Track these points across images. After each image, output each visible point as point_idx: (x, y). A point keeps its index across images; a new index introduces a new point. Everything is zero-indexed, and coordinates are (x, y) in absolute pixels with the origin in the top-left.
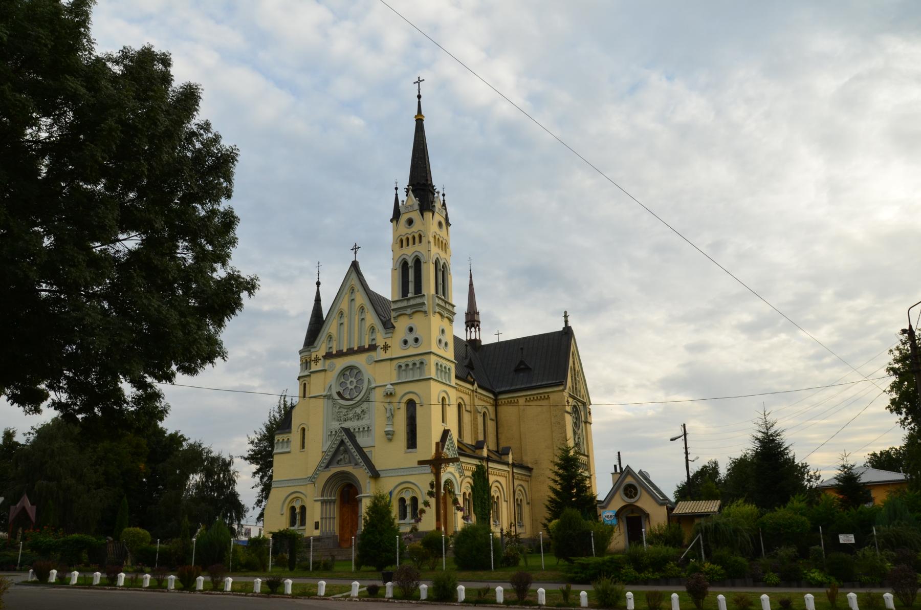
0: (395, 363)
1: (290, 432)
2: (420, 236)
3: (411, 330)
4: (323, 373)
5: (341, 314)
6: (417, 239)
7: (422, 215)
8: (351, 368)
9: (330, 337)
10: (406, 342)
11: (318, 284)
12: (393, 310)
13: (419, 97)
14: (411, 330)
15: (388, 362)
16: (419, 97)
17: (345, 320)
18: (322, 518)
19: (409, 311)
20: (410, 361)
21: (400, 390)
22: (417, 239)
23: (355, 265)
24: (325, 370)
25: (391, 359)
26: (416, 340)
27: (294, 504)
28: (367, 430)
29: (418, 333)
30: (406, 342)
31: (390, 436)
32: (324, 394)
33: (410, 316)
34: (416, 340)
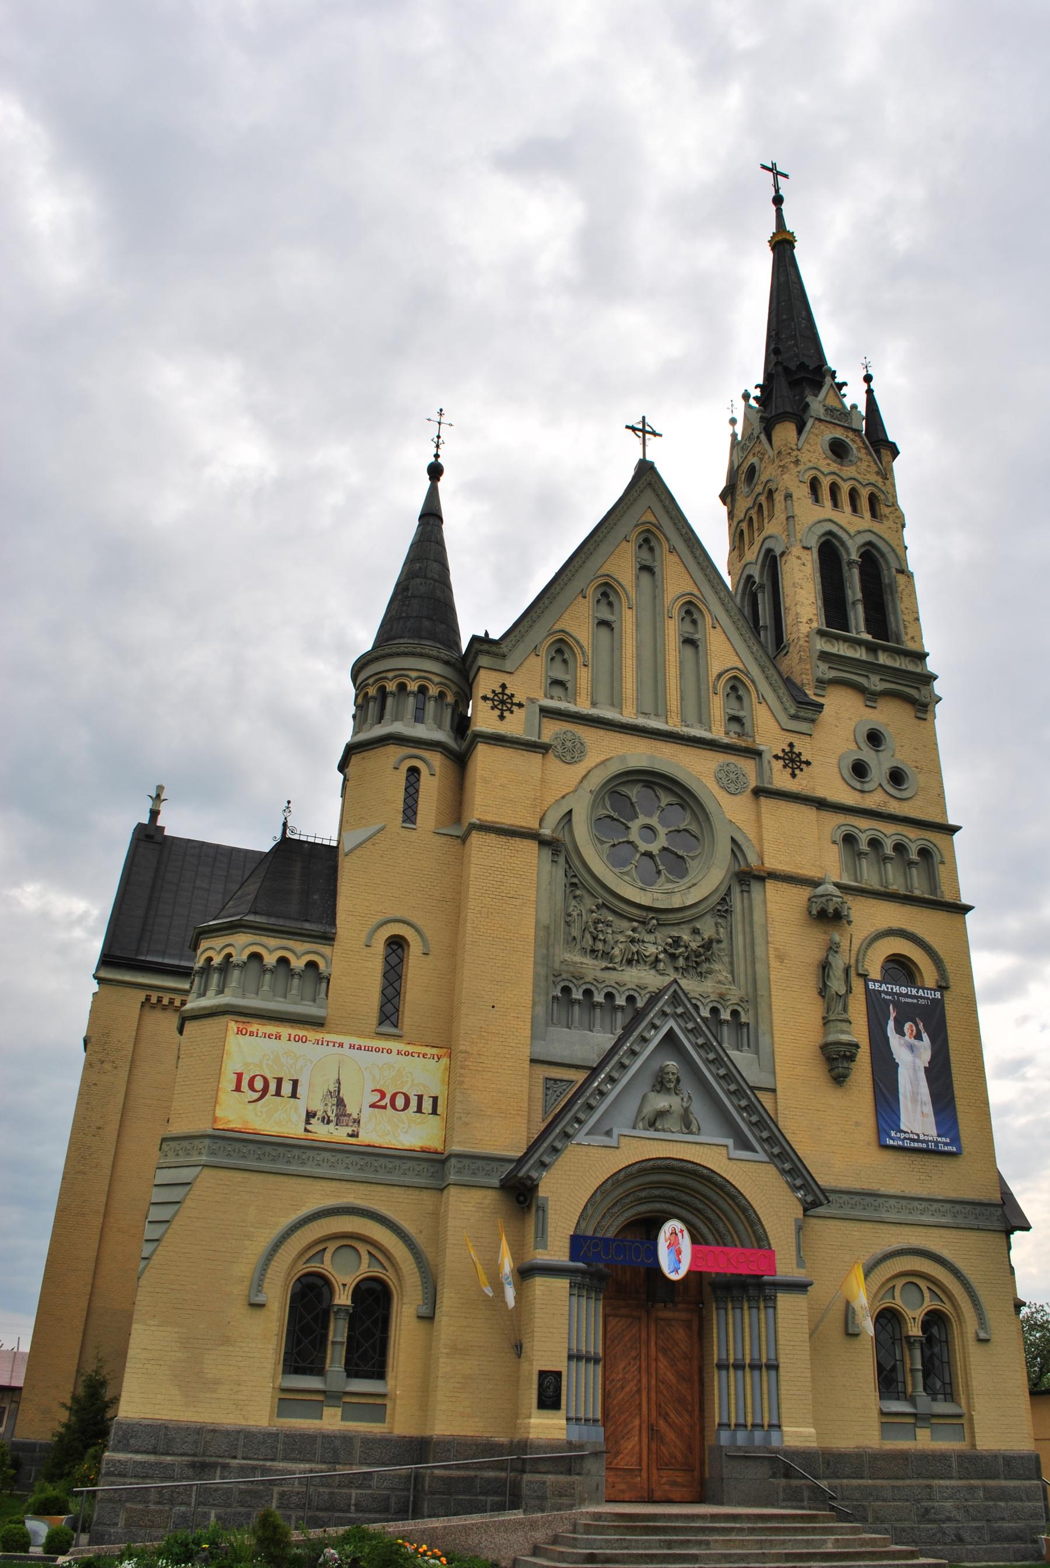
0: (834, 822)
1: (328, 938)
2: (873, 499)
3: (875, 738)
4: (536, 758)
5: (607, 593)
6: (864, 504)
7: (878, 452)
8: (653, 780)
9: (562, 649)
10: (860, 770)
11: (435, 471)
12: (824, 656)
13: (778, 200)
14: (875, 738)
15: (809, 814)
16: (778, 200)
17: (628, 620)
18: (570, 1357)
19: (875, 683)
20: (890, 833)
21: (868, 917)
22: (864, 504)
23: (645, 471)
24: (541, 748)
25: (821, 804)
26: (897, 777)
27: (327, 1266)
28: (739, 1023)
29: (899, 751)
30: (860, 770)
31: (836, 1060)
32: (546, 832)
33: (871, 697)
34: (897, 777)
